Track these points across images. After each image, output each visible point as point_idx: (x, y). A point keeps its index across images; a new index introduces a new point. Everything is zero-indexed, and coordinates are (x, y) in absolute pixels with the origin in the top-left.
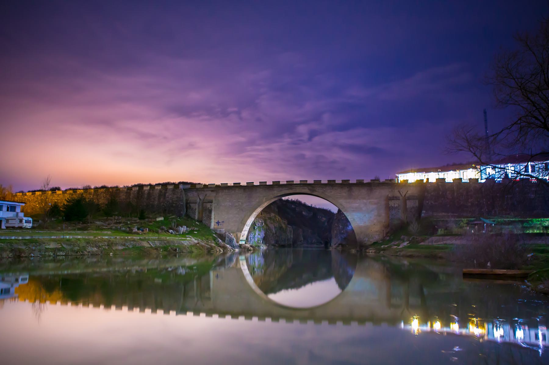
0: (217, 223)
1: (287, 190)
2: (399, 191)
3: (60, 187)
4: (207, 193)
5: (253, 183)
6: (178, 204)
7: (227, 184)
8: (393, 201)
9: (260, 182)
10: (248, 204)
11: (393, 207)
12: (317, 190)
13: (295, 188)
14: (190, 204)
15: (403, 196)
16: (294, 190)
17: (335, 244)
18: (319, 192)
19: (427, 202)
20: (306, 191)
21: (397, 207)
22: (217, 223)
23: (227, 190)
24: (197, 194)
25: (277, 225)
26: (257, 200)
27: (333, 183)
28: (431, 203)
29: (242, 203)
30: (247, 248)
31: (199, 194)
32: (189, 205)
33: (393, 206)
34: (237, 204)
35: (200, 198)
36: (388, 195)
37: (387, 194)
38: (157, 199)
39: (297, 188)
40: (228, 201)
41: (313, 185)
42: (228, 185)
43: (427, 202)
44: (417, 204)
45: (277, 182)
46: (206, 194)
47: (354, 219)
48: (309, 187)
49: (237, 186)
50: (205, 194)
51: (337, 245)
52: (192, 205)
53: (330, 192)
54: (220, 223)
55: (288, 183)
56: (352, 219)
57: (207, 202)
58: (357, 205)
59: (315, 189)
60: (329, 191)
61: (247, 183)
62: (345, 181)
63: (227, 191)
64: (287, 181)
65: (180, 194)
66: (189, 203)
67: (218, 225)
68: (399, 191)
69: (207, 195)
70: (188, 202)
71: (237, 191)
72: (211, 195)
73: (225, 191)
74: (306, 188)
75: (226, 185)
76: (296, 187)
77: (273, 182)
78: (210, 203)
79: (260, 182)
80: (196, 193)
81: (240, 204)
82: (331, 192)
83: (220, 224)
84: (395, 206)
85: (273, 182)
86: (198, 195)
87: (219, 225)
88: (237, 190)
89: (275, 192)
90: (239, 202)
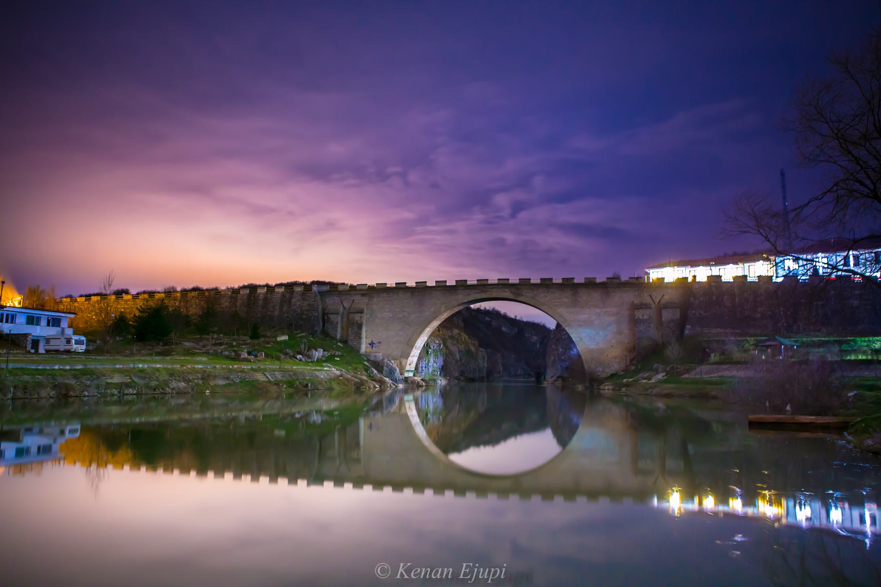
0: (370, 344)
1: (479, 293)
3: (128, 288)
4: (354, 298)
5: (426, 282)
6: (310, 315)
7: (386, 284)
8: (641, 310)
9: (436, 282)
10: (417, 315)
11: (640, 319)
12: (524, 294)
13: (490, 290)
14: (328, 315)
15: (657, 303)
16: (489, 293)
17: (552, 377)
18: (527, 296)
19: (694, 312)
20: (508, 294)
21: (646, 319)
22: (370, 344)
24: (340, 300)
25: (462, 347)
26: (432, 309)
27: (549, 283)
28: (700, 314)
29: (408, 314)
30: (417, 382)
31: (342, 299)
32: (327, 316)
33: (641, 317)
34: (401, 315)
35: (344, 305)
36: (633, 301)
37: (632, 300)
38: (277, 307)
40: (387, 310)
41: (519, 287)
42: (388, 286)
43: (694, 312)
44: (678, 315)
45: (463, 282)
47: (581, 339)
48: (512, 290)
49: (401, 287)
51: (554, 378)
52: (331, 316)
53: (543, 296)
54: (375, 344)
55: (479, 283)
56: (578, 339)
57: (355, 311)
58: (586, 316)
59: (521, 291)
60: (542, 295)
61: (416, 283)
62: (567, 279)
63: (385, 295)
64: (478, 280)
65: (313, 300)
66: (327, 314)
68: (650, 296)
69: (355, 302)
70: (326, 312)
71: (401, 296)
72: (361, 302)
73: (382, 295)
74: (507, 290)
75: (384, 286)
76: (492, 288)
79: (436, 282)
80: (338, 298)
81: (407, 315)
83: (374, 345)
84: (645, 318)
88: (401, 294)
89: (460, 296)
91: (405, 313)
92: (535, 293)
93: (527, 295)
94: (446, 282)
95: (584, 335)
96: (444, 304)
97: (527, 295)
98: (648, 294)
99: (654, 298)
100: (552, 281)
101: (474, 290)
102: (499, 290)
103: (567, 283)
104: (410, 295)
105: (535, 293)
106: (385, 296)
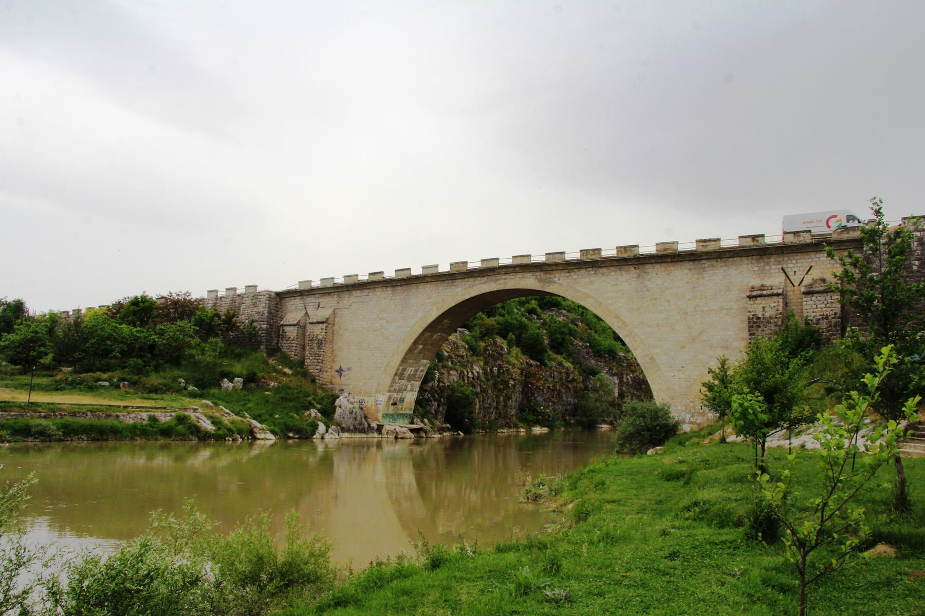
0: (337, 371)
1: (485, 283)
2: (782, 269)
3: (24, 300)
4: (320, 300)
5: (409, 269)
8: (759, 300)
9: (423, 268)
11: (758, 318)
12: (556, 279)
13: (503, 277)
14: (285, 328)
15: (796, 284)
16: (502, 281)
18: (561, 285)
21: (771, 318)
22: (337, 371)
23: (358, 292)
24: (303, 305)
29: (387, 322)
32: (283, 330)
33: (760, 315)
35: (308, 312)
39: (508, 276)
40: (360, 317)
41: (547, 268)
42: (360, 278)
45: (461, 265)
46: (319, 303)
47: (652, 359)
48: (538, 274)
50: (317, 304)
52: (287, 329)
56: (647, 359)
59: (553, 276)
60: (587, 280)
62: (625, 248)
64: (482, 261)
65: (264, 305)
66: (283, 325)
67: (340, 377)
68: (782, 269)
69: (320, 306)
71: (378, 293)
72: (324, 309)
74: (529, 275)
77: (451, 265)
78: (320, 325)
79: (423, 268)
80: (301, 302)
82: (591, 282)
84: (767, 315)
85: (451, 265)
86: (304, 306)
87: (342, 377)
89: (459, 290)
90: (381, 319)
91: (385, 321)
92: (575, 277)
93: (560, 282)
94: (437, 266)
96: (436, 304)
97: (560, 282)
98: (780, 267)
99: (791, 274)
100: (600, 253)
101: (479, 279)
102: (518, 276)
103: (625, 255)
104: (390, 292)
105: (575, 277)
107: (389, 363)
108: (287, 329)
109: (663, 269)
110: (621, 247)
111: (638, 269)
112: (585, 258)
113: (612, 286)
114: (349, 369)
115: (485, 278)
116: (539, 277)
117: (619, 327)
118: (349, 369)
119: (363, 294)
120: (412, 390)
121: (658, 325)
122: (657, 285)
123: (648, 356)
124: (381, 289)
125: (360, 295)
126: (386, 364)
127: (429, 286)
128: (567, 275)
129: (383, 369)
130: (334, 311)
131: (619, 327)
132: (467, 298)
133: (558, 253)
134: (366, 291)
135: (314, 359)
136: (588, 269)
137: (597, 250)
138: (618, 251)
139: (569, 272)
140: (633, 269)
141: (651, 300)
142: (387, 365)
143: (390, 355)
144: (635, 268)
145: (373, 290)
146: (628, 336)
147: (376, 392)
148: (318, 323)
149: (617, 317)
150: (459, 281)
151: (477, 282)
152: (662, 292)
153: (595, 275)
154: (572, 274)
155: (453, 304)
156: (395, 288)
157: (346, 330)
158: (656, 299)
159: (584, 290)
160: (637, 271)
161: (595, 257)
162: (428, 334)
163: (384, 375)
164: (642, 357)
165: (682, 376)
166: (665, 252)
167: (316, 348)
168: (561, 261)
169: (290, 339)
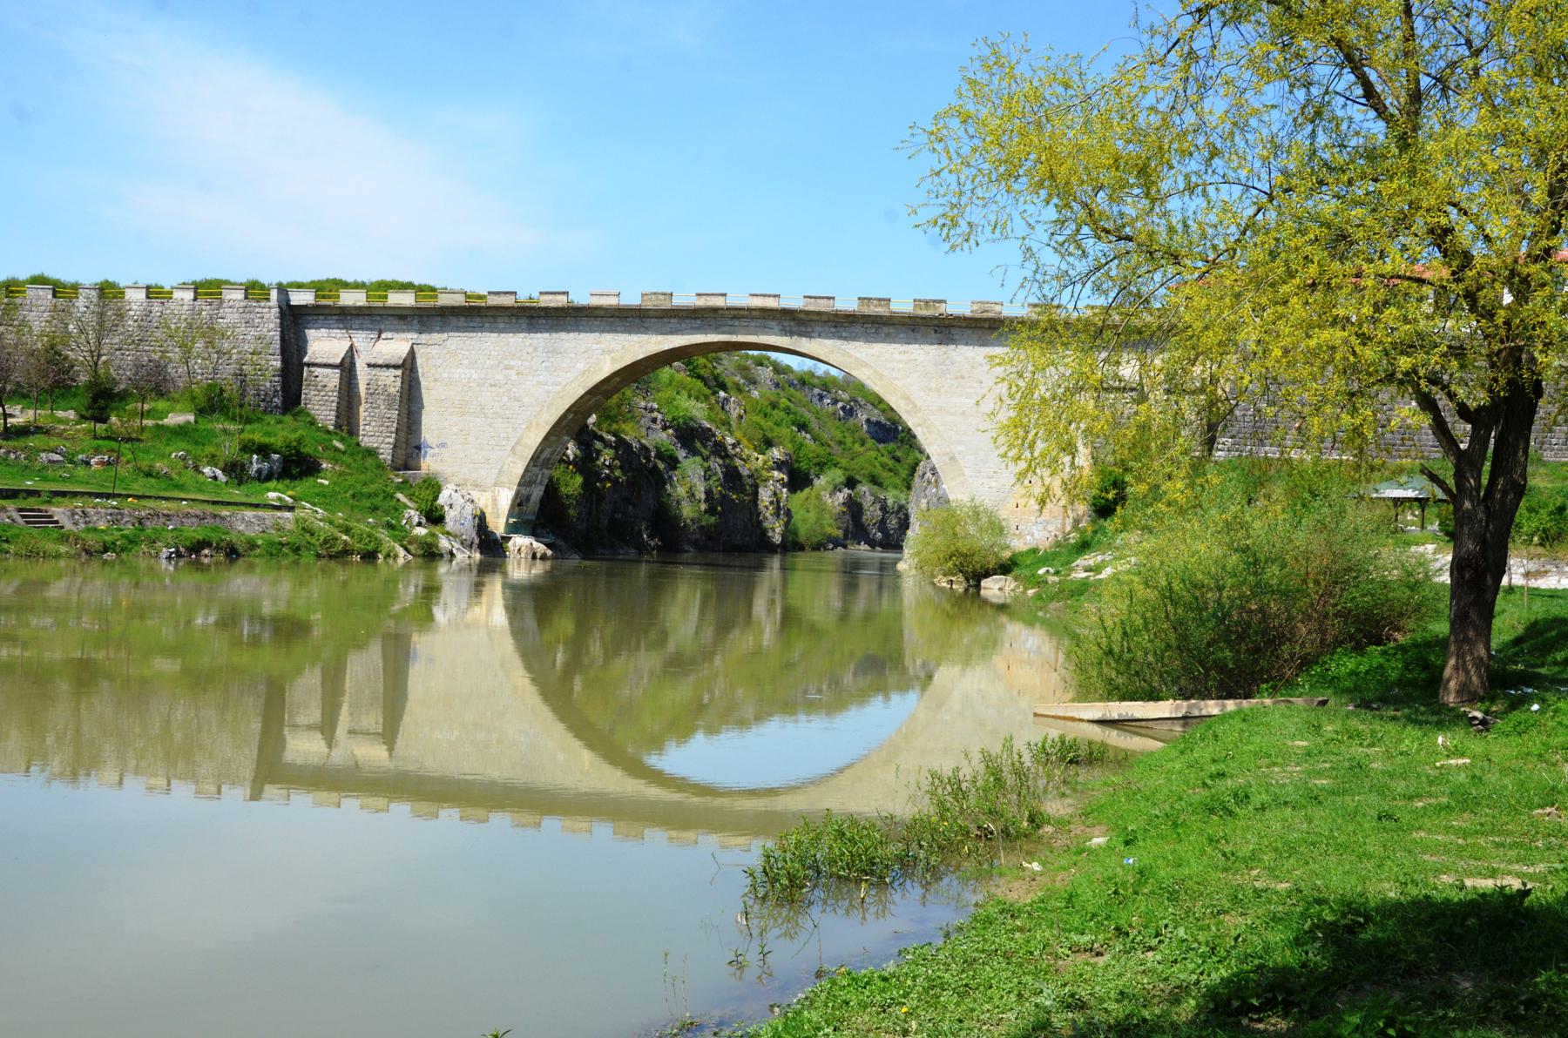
10: (541, 378)
13: (730, 322)
23: (462, 319)
39: (737, 323)
40: (467, 362)
45: (661, 297)
47: (953, 458)
56: (946, 459)
59: (810, 330)
66: (309, 365)
78: (391, 370)
81: (514, 377)
91: (512, 373)
95: (961, 448)
96: (610, 352)
100: (888, 306)
102: (753, 324)
104: (524, 326)
105: (844, 334)
106: (460, 324)
107: (520, 439)
108: (318, 371)
109: (976, 337)
110: (920, 301)
111: (941, 333)
112: (866, 310)
113: (900, 353)
114: (443, 445)
115: (698, 322)
116: (788, 329)
117: (907, 412)
118: (443, 445)
119: (471, 325)
120: (540, 483)
121: (963, 413)
122: (967, 359)
123: (947, 454)
124: (507, 320)
125: (466, 324)
126: (514, 440)
127: (598, 323)
128: (833, 330)
129: (509, 448)
130: (412, 348)
131: (907, 412)
132: (666, 348)
133: (823, 298)
134: (478, 319)
135: (382, 426)
136: (866, 326)
137: (884, 300)
138: (915, 306)
139: (835, 327)
140: (933, 332)
141: (956, 378)
142: (517, 443)
143: (524, 426)
144: (936, 331)
145: (491, 320)
146: (919, 425)
147: (495, 485)
148: (388, 366)
149: (907, 398)
150: (653, 320)
151: (684, 326)
152: (973, 368)
153: (875, 335)
154: (841, 329)
155: (641, 356)
156: (534, 321)
157: (436, 380)
158: (963, 378)
159: (858, 355)
160: (938, 335)
161: (880, 310)
162: (588, 396)
163: (510, 459)
164: (938, 455)
165: (994, 484)
166: (985, 315)
167: (382, 407)
168: (828, 309)
169: (327, 389)
